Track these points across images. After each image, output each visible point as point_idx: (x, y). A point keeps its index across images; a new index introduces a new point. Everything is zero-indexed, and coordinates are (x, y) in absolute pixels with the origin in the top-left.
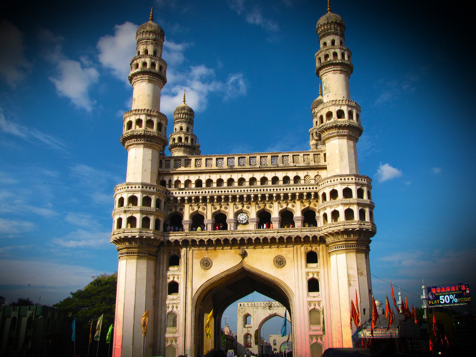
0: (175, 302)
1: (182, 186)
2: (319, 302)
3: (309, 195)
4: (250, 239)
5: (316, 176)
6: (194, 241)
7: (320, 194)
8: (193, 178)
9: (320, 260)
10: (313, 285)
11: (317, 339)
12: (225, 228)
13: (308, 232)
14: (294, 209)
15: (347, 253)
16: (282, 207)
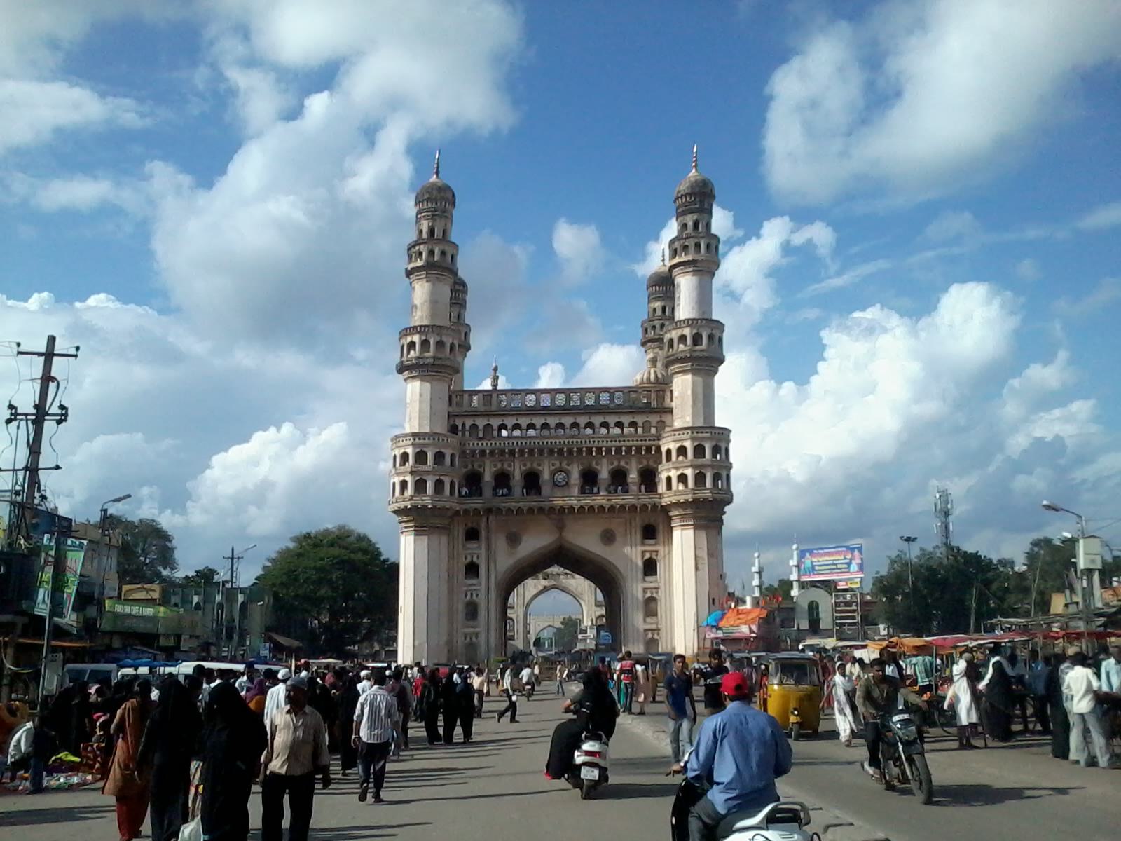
0: (475, 588)
1: (481, 434)
2: (657, 588)
3: (649, 449)
4: (572, 508)
5: (658, 422)
6: (499, 510)
7: (664, 449)
8: (495, 422)
9: (660, 536)
10: (650, 567)
11: (653, 634)
12: (538, 491)
13: (646, 500)
14: (627, 467)
15: (695, 529)
16: (612, 464)
